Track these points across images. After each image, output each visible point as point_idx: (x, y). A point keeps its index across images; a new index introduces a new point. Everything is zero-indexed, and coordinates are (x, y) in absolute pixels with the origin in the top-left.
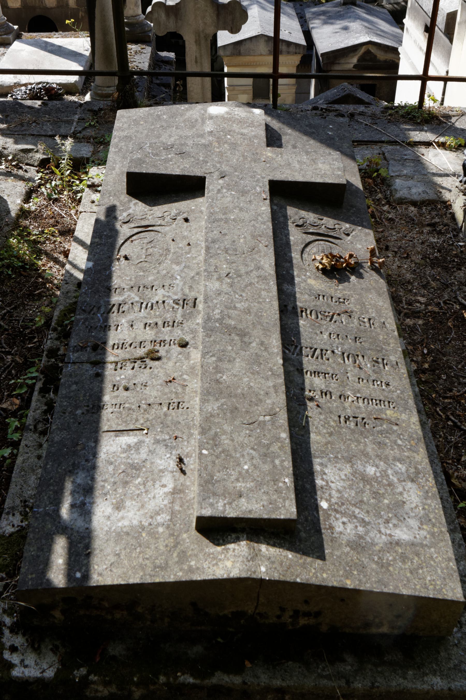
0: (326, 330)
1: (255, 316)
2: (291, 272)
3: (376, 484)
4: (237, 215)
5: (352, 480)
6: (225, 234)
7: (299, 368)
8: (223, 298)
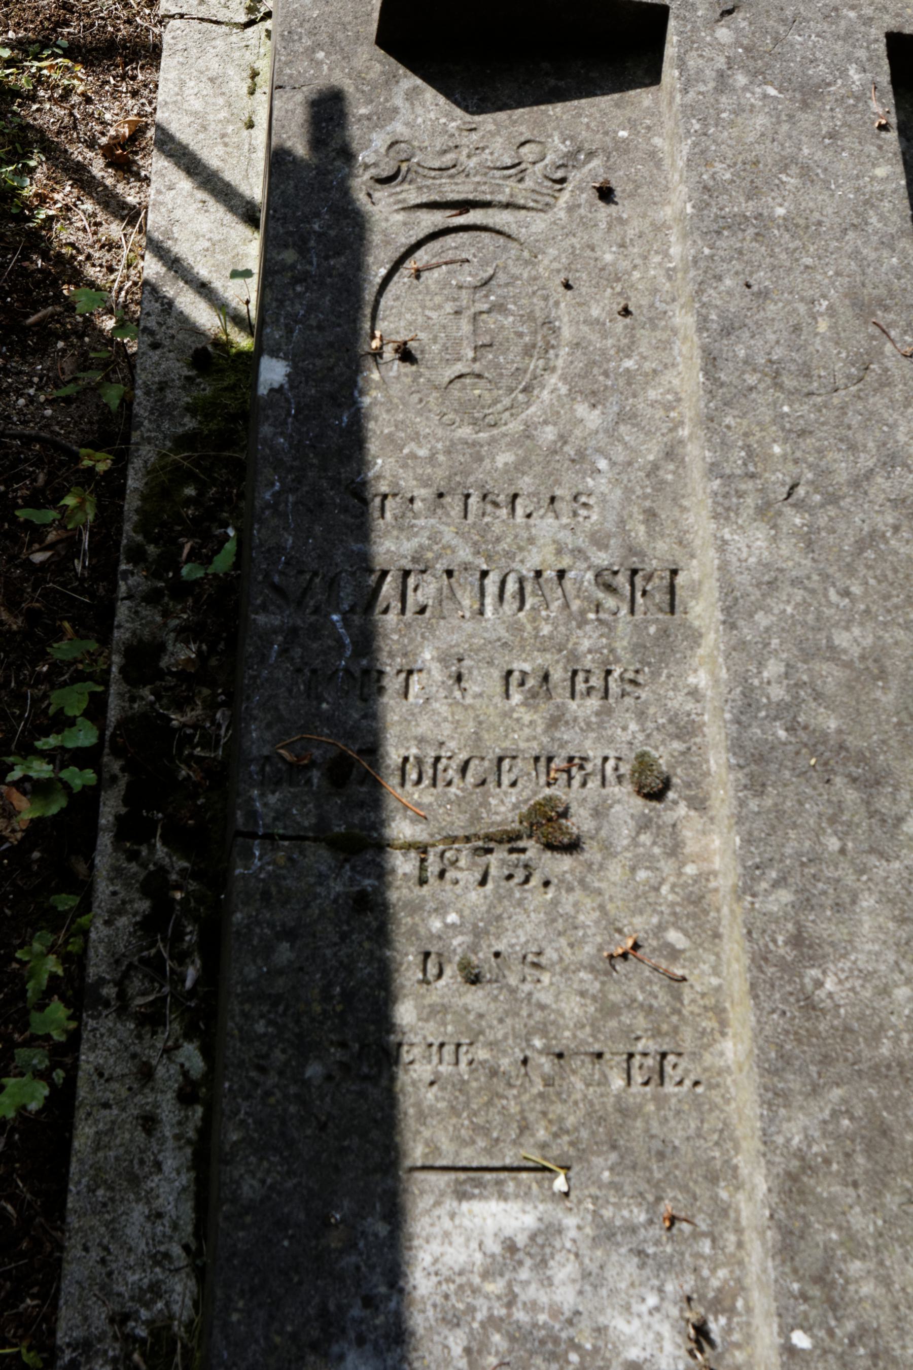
6: (764, 295)
8: (786, 603)
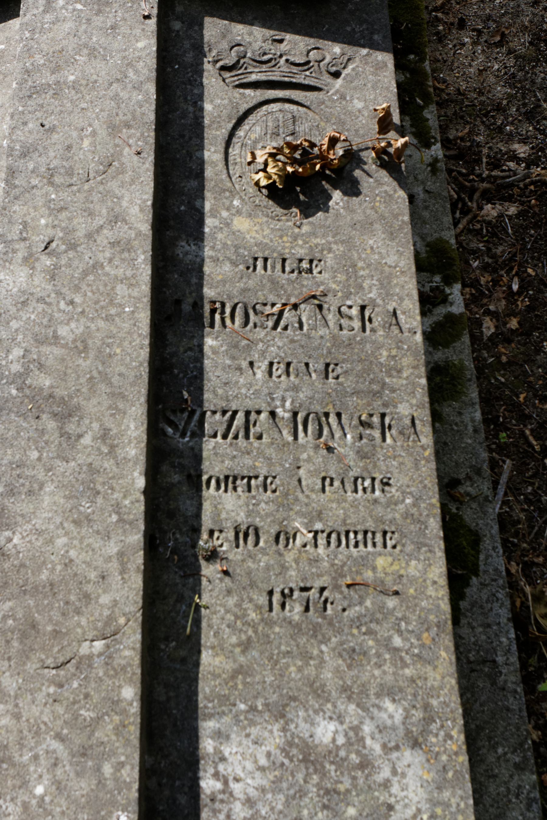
0: (263, 353)
1: (97, 357)
2: (198, 204)
3: (333, 767)
4: (83, 71)
5: (283, 764)
6: (52, 130)
7: (192, 472)
8: (32, 314)
